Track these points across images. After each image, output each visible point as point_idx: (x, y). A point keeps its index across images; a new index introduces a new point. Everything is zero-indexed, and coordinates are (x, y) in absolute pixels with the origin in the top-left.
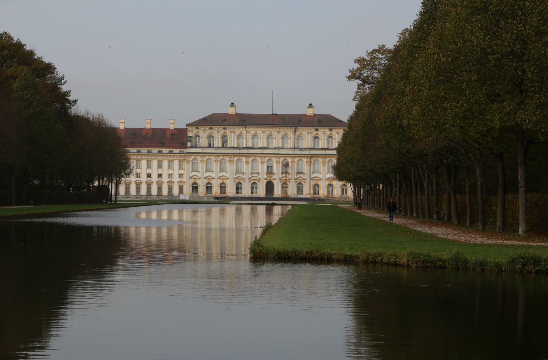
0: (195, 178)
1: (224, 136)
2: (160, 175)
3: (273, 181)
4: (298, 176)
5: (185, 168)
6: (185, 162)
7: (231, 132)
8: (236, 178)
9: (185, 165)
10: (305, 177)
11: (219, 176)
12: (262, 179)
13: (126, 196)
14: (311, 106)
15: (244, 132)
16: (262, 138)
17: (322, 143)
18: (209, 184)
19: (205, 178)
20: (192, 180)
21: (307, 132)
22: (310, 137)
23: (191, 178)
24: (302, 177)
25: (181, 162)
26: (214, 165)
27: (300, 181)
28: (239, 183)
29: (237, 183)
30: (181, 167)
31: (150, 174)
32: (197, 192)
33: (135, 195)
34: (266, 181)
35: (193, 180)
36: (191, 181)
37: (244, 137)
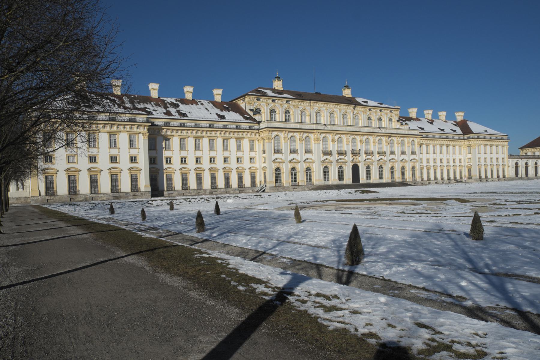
1: (287, 112)
2: (226, 160)
3: (358, 164)
5: (257, 150)
6: (257, 142)
8: (323, 161)
11: (304, 159)
13: (185, 192)
17: (375, 123)
20: (275, 164)
21: (363, 112)
23: (274, 161)
25: (251, 141)
30: (251, 149)
31: (170, 158)
32: (280, 181)
34: (352, 164)
35: (276, 165)
36: (273, 167)
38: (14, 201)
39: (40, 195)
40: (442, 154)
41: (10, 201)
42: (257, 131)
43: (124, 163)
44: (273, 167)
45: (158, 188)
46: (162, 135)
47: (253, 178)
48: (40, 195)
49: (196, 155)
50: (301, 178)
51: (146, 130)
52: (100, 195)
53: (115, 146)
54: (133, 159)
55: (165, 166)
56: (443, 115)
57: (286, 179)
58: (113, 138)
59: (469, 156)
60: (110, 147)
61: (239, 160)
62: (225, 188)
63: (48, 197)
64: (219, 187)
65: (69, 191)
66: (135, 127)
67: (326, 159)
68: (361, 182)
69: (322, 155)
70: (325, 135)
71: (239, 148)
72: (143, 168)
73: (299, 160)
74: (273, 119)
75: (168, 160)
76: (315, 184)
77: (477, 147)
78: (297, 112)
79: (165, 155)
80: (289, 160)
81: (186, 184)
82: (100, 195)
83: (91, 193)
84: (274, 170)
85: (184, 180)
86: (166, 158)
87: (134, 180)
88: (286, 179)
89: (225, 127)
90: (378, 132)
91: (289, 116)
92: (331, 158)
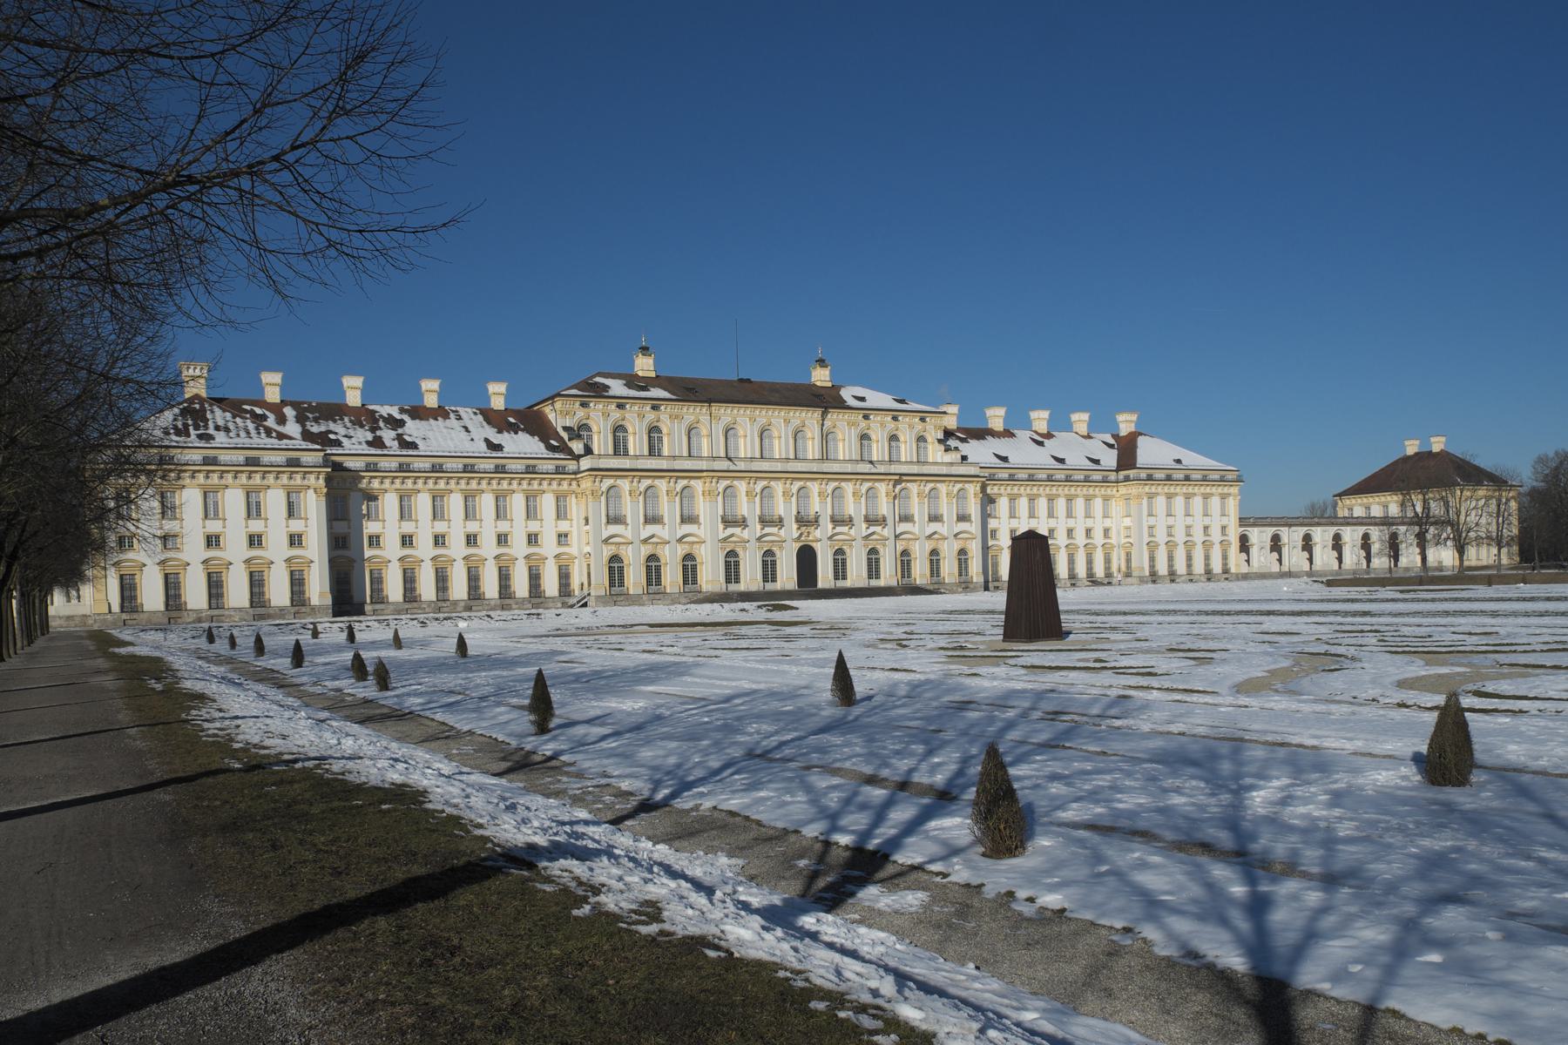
0: (616, 544)
1: (653, 430)
2: (502, 539)
3: (814, 545)
4: (870, 531)
5: (574, 518)
7: (673, 417)
8: (725, 540)
9: (572, 502)
10: (886, 532)
11: (679, 535)
12: (789, 540)
14: (822, 362)
15: (705, 419)
16: (748, 435)
18: (652, 558)
19: (645, 541)
22: (854, 434)
23: (606, 541)
24: (878, 534)
25: (560, 498)
26: (701, 504)
27: (875, 542)
28: (732, 554)
29: (727, 555)
30: (561, 514)
33: (435, 599)
37: (704, 431)
38: (62, 622)
39: (110, 612)
40: (1034, 517)
41: (52, 623)
42: (573, 476)
43: (276, 549)
44: (605, 554)
45: (351, 597)
46: (361, 490)
47: (564, 577)
48: (110, 612)
49: (434, 530)
50: (671, 577)
51: (322, 482)
52: (227, 613)
53: (259, 514)
54: (295, 540)
55: (368, 553)
56: (1080, 420)
57: (634, 578)
58: (253, 499)
59: (1127, 522)
60: (249, 516)
61: (532, 539)
62: (500, 598)
63: (124, 616)
64: (487, 596)
65: (167, 605)
66: (298, 477)
67: (732, 535)
68: (820, 585)
69: (721, 526)
70: (728, 482)
71: (531, 513)
72: (316, 559)
73: (667, 538)
74: (619, 448)
75: (375, 541)
76: (704, 590)
77: (1145, 502)
78: (680, 430)
79: (368, 531)
80: (642, 538)
81: (413, 589)
82: (227, 613)
83: (210, 608)
84: (605, 559)
85: (409, 581)
86: (370, 537)
87: (297, 583)
88: (634, 578)
89: (500, 469)
90: (867, 471)
91: (660, 439)
92: (746, 534)
